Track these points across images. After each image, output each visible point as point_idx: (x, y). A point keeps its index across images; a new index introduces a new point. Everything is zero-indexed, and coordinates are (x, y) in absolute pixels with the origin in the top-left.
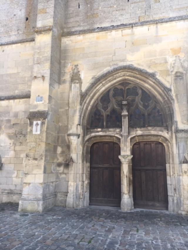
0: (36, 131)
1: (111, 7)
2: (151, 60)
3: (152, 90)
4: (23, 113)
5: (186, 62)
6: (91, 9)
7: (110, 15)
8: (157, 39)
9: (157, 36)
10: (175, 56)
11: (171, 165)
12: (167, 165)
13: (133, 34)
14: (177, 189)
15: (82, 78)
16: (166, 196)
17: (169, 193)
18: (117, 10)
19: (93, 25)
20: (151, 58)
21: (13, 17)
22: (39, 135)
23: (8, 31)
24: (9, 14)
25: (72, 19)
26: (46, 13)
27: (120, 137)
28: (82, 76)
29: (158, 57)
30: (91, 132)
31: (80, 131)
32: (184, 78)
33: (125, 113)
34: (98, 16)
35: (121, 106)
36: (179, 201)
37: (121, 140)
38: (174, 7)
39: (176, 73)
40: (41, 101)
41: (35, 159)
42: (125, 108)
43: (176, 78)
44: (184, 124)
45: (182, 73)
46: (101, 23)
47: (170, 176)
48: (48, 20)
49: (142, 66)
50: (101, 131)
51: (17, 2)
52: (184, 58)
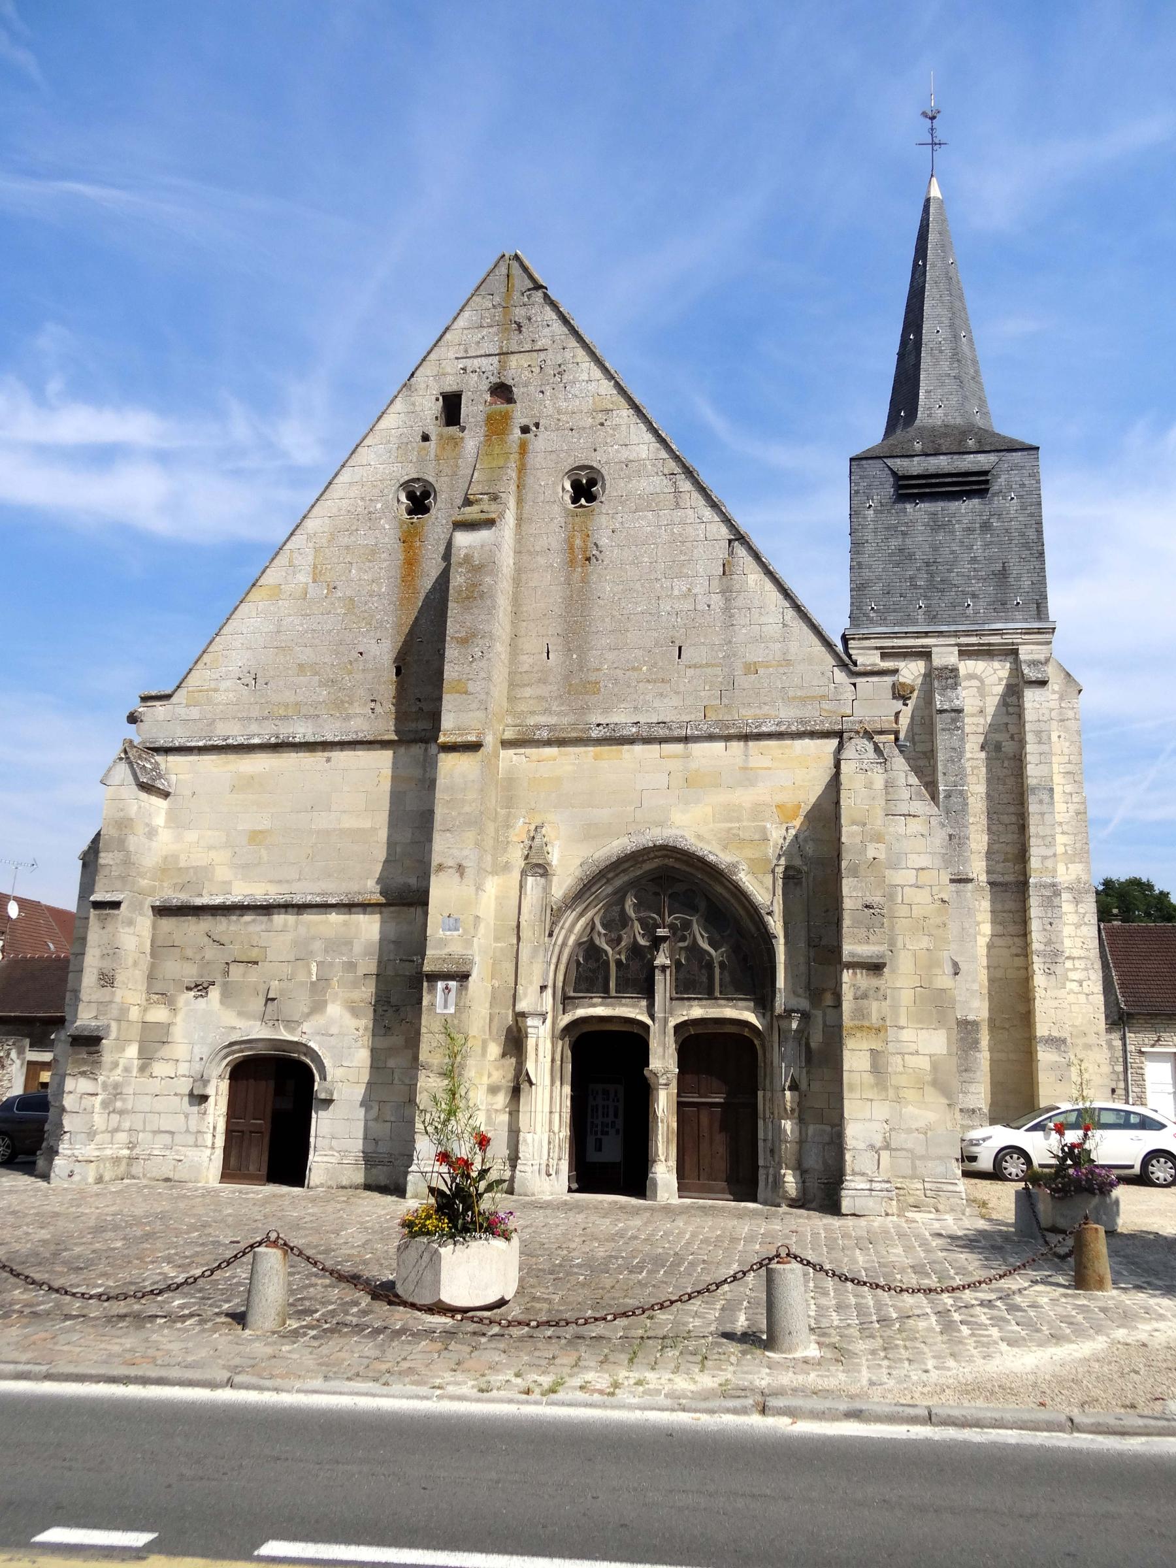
0: (446, 1007)
1: (634, 669)
2: (731, 829)
3: (733, 901)
4: (392, 946)
5: (810, 843)
6: (581, 670)
7: (632, 690)
8: (748, 776)
10: (785, 826)
11: (769, 1094)
12: (760, 1094)
14: (776, 1150)
15: (555, 863)
17: (761, 1162)
18: (648, 681)
19: (585, 714)
21: (356, 660)
23: (342, 702)
24: (342, 648)
25: (528, 689)
26: (466, 693)
27: (649, 1021)
28: (555, 857)
29: (745, 824)
31: (548, 1001)
32: (804, 884)
33: (662, 959)
34: (599, 690)
35: (657, 942)
37: (652, 1029)
38: (791, 694)
40: (457, 929)
42: (665, 946)
44: (799, 996)
45: (799, 871)
46: (606, 711)
48: (471, 714)
49: (708, 843)
50: (601, 1005)
51: (366, 615)
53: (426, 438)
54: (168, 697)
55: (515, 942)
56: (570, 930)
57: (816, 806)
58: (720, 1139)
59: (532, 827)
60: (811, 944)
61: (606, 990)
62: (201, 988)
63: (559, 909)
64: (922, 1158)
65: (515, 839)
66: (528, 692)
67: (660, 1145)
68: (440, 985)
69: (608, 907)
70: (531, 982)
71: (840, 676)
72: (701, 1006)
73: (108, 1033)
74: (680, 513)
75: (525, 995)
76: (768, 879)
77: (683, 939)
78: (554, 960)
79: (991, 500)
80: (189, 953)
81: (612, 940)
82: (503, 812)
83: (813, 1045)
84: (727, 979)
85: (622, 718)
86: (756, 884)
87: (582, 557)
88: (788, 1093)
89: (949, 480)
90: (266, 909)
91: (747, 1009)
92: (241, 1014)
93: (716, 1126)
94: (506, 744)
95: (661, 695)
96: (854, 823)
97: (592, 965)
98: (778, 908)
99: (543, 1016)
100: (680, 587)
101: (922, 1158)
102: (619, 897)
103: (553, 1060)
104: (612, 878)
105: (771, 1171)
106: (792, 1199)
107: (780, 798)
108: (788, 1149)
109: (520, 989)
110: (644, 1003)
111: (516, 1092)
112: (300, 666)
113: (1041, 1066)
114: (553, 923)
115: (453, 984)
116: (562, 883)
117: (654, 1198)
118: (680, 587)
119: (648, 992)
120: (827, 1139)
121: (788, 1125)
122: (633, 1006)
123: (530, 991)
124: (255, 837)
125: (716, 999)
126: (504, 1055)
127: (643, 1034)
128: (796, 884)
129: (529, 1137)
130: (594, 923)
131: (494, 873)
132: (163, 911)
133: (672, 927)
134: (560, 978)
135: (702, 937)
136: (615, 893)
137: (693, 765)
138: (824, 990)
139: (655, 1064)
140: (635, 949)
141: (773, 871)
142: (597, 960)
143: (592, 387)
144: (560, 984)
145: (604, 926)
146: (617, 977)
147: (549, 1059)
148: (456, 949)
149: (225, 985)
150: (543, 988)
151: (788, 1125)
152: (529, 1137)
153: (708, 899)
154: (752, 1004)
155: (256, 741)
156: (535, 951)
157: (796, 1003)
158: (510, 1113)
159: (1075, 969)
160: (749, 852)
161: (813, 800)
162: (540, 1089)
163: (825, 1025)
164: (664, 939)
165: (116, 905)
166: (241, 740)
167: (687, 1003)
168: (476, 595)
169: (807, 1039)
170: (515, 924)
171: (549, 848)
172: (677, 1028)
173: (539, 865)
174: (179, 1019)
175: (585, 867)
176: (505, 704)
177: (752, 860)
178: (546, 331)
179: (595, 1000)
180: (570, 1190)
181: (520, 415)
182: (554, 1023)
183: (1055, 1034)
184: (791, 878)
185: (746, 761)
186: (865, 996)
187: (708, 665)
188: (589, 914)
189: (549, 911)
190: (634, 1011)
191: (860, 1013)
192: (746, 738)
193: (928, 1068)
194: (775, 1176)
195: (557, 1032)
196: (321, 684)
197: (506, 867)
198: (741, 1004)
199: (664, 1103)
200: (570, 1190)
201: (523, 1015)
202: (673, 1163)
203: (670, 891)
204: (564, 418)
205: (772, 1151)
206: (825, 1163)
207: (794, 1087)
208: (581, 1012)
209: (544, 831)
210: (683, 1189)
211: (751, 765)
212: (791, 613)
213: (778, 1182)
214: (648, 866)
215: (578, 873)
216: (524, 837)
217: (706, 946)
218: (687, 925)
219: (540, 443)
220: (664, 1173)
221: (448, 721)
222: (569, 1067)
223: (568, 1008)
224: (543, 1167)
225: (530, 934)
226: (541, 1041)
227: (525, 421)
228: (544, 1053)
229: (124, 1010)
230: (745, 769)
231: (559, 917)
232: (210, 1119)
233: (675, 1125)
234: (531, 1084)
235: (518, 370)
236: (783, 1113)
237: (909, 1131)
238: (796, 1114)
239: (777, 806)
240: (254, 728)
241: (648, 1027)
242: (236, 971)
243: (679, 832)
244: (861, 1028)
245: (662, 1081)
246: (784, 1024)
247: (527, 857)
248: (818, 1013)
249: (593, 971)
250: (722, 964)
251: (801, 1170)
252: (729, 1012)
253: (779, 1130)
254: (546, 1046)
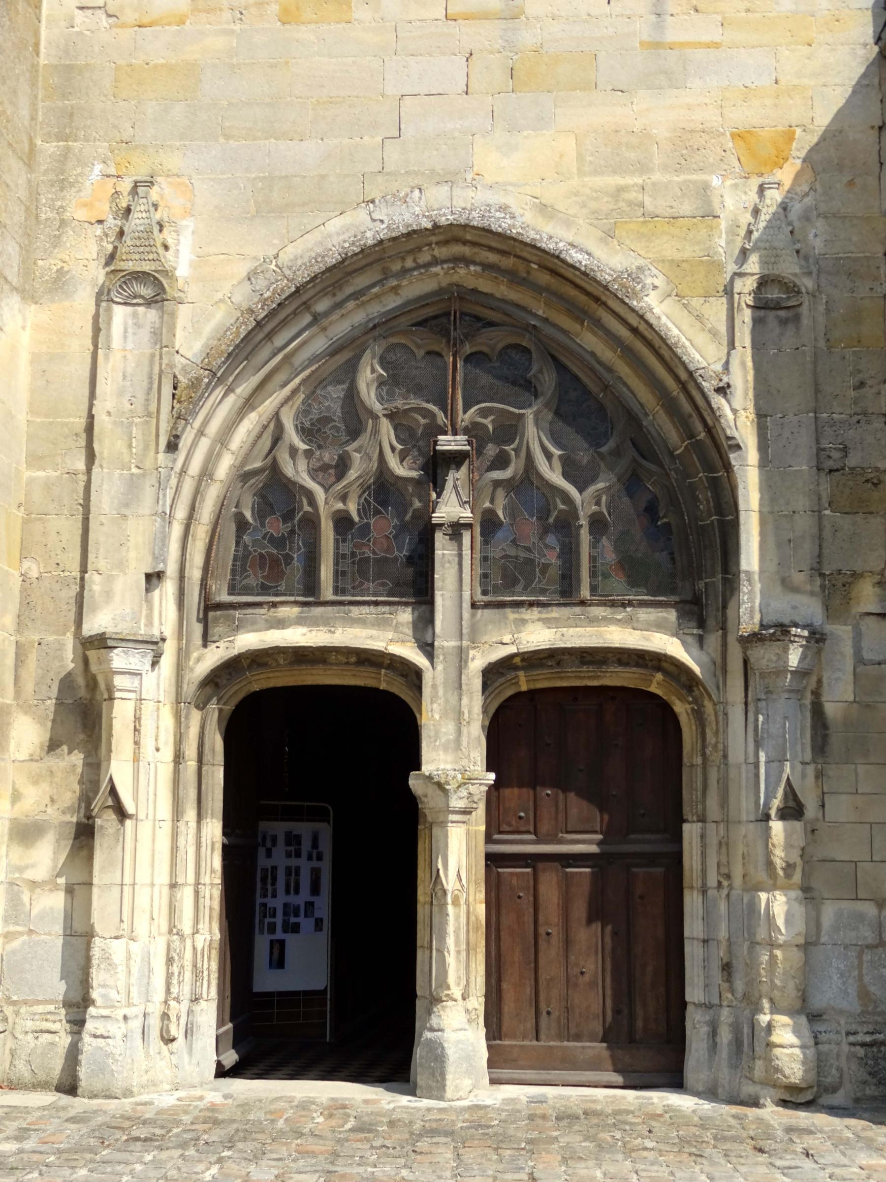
2: (621, 189)
3: (624, 370)
5: (820, 224)
10: (755, 182)
11: (714, 833)
14: (739, 966)
16: (676, 1006)
17: (694, 993)
20: (619, 180)
28: (182, 260)
29: (657, 177)
32: (805, 321)
35: (436, 467)
36: (746, 1030)
42: (456, 477)
43: (762, 313)
44: (795, 590)
45: (793, 289)
47: (704, 891)
49: (568, 223)
50: (300, 621)
52: (807, 194)
55: (81, 466)
56: (223, 439)
57: (833, 136)
58: (589, 938)
59: (126, 186)
60: (825, 466)
61: (311, 587)
63: (195, 384)
65: (81, 214)
67: (451, 960)
69: (315, 386)
70: (121, 565)
72: (548, 623)
75: (108, 595)
76: (717, 311)
77: (501, 462)
78: (181, 513)
81: (325, 468)
82: (49, 148)
83: (831, 709)
84: (609, 554)
86: (686, 320)
88: (777, 827)
91: (660, 626)
93: (580, 909)
97: (276, 527)
98: (742, 378)
99: (153, 646)
102: (344, 359)
103: (178, 758)
104: (327, 314)
105: (725, 1015)
106: (792, 1088)
107: (743, 115)
108: (777, 965)
109: (95, 583)
110: (406, 616)
111: (84, 835)
114: (180, 418)
116: (202, 324)
117: (438, 1090)
119: (419, 589)
120: (868, 935)
121: (778, 905)
122: (381, 623)
123: (119, 585)
125: (583, 603)
126: (53, 746)
127: (405, 695)
128: (784, 322)
129: (117, 949)
130: (279, 428)
133: (473, 431)
134: (197, 558)
135: (549, 456)
136: (334, 351)
137: (527, 38)
138: (856, 576)
139: (435, 760)
140: (383, 490)
141: (729, 291)
142: (288, 516)
144: (195, 574)
145: (305, 432)
146: (339, 558)
147: (167, 754)
150: (153, 578)
151: (778, 905)
152: (117, 949)
153: (561, 367)
154: (671, 615)
156: (133, 485)
157: (784, 606)
158: (70, 890)
160: (669, 248)
161: (823, 118)
162: (145, 829)
163: (859, 660)
164: (456, 459)
167: (511, 615)
169: (817, 694)
170: (80, 422)
171: (168, 235)
172: (493, 674)
173: (140, 276)
175: (261, 283)
177: (677, 264)
179: (284, 611)
180: (222, 1072)
182: (180, 668)
184: (775, 304)
185: (659, 26)
188: (268, 406)
189: (167, 390)
190: (378, 632)
194: (736, 1029)
195: (190, 689)
197: (60, 283)
198: (645, 615)
199: (457, 856)
200: (222, 1072)
201: (101, 643)
202: (477, 1002)
203: (468, 349)
205: (727, 968)
206: (864, 994)
207: (792, 810)
208: (249, 640)
209: (154, 194)
210: (501, 1063)
211: (672, 35)
213: (749, 1044)
214: (416, 287)
215: (243, 296)
216: (104, 210)
217: (555, 477)
218: (509, 430)
220: (456, 1024)
222: (217, 776)
223: (216, 630)
224: (155, 1023)
225: (120, 445)
226: (148, 708)
228: (160, 749)
230: (656, 45)
231: (195, 404)
234: (122, 814)
236: (762, 875)
238: (797, 877)
239: (737, 136)
243: (495, 198)
245: (457, 802)
246: (763, 656)
247: (111, 258)
248: (842, 632)
249: (278, 542)
250: (598, 524)
251: (811, 1015)
252: (618, 634)
253: (750, 916)
254: (160, 724)
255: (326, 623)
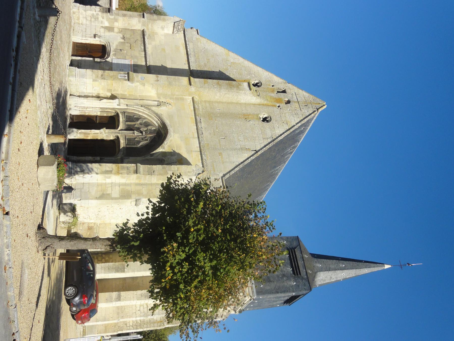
9: (192, 151)
13: (194, 138)
22: (118, 78)
30: (122, 115)
31: (123, 107)
35: (142, 132)
38: (214, 163)
39: (164, 160)
41: (102, 75)
53: (273, 86)
54: (198, 34)
61: (127, 121)
62: (124, 38)
64: (81, 191)
66: (208, 105)
68: (127, 75)
71: (222, 175)
73: (111, 15)
74: (262, 139)
79: (292, 277)
80: (132, 36)
85: (202, 125)
87: (246, 117)
89: (296, 264)
90: (145, 51)
92: (117, 45)
94: (193, 98)
95: (210, 134)
96: (178, 168)
100: (241, 139)
101: (81, 191)
109: (126, 100)
112: (209, 59)
113: (111, 293)
115: (127, 78)
118: (241, 139)
124: (164, 50)
131: (158, 94)
132: (143, 31)
143: (293, 121)
145: (145, 122)
148: (136, 79)
149: (124, 43)
155: (188, 50)
159: (144, 308)
165: (144, 17)
166: (188, 47)
168: (231, 87)
174: (115, 34)
176: (203, 100)
178: (306, 111)
181: (283, 105)
183: (122, 298)
185: (194, 151)
186: (128, 169)
187: (220, 144)
190: (121, 126)
191: (123, 168)
192: (201, 151)
193: (108, 193)
196: (205, 64)
197: (159, 98)
204: (283, 114)
208: (120, 115)
212: (238, 164)
219: (276, 109)
221: (197, 80)
222: (105, 115)
227: (281, 106)
229: (116, 20)
232: (89, 39)
233: (89, 138)
235: (294, 105)
237: (89, 188)
240: (192, 50)
241: (117, 129)
242: (129, 45)
243: (172, 136)
244: (118, 168)
255: (123, 122)
